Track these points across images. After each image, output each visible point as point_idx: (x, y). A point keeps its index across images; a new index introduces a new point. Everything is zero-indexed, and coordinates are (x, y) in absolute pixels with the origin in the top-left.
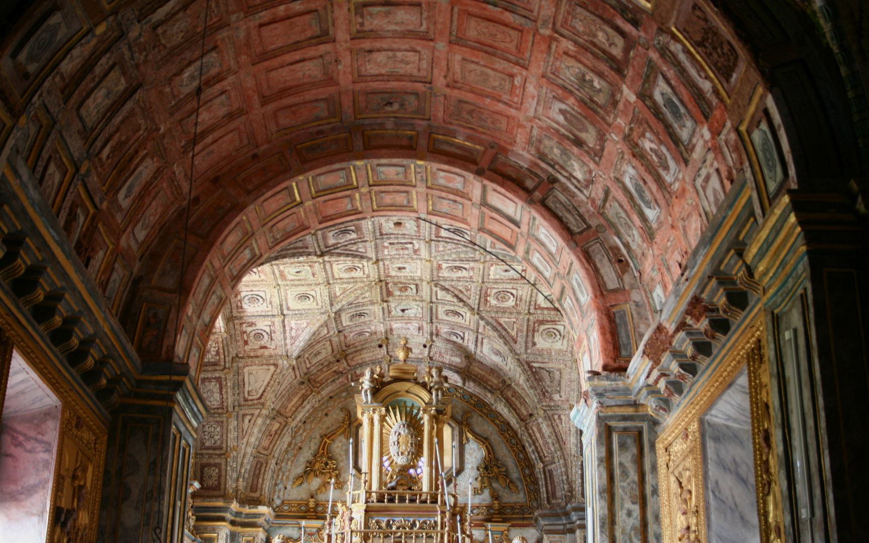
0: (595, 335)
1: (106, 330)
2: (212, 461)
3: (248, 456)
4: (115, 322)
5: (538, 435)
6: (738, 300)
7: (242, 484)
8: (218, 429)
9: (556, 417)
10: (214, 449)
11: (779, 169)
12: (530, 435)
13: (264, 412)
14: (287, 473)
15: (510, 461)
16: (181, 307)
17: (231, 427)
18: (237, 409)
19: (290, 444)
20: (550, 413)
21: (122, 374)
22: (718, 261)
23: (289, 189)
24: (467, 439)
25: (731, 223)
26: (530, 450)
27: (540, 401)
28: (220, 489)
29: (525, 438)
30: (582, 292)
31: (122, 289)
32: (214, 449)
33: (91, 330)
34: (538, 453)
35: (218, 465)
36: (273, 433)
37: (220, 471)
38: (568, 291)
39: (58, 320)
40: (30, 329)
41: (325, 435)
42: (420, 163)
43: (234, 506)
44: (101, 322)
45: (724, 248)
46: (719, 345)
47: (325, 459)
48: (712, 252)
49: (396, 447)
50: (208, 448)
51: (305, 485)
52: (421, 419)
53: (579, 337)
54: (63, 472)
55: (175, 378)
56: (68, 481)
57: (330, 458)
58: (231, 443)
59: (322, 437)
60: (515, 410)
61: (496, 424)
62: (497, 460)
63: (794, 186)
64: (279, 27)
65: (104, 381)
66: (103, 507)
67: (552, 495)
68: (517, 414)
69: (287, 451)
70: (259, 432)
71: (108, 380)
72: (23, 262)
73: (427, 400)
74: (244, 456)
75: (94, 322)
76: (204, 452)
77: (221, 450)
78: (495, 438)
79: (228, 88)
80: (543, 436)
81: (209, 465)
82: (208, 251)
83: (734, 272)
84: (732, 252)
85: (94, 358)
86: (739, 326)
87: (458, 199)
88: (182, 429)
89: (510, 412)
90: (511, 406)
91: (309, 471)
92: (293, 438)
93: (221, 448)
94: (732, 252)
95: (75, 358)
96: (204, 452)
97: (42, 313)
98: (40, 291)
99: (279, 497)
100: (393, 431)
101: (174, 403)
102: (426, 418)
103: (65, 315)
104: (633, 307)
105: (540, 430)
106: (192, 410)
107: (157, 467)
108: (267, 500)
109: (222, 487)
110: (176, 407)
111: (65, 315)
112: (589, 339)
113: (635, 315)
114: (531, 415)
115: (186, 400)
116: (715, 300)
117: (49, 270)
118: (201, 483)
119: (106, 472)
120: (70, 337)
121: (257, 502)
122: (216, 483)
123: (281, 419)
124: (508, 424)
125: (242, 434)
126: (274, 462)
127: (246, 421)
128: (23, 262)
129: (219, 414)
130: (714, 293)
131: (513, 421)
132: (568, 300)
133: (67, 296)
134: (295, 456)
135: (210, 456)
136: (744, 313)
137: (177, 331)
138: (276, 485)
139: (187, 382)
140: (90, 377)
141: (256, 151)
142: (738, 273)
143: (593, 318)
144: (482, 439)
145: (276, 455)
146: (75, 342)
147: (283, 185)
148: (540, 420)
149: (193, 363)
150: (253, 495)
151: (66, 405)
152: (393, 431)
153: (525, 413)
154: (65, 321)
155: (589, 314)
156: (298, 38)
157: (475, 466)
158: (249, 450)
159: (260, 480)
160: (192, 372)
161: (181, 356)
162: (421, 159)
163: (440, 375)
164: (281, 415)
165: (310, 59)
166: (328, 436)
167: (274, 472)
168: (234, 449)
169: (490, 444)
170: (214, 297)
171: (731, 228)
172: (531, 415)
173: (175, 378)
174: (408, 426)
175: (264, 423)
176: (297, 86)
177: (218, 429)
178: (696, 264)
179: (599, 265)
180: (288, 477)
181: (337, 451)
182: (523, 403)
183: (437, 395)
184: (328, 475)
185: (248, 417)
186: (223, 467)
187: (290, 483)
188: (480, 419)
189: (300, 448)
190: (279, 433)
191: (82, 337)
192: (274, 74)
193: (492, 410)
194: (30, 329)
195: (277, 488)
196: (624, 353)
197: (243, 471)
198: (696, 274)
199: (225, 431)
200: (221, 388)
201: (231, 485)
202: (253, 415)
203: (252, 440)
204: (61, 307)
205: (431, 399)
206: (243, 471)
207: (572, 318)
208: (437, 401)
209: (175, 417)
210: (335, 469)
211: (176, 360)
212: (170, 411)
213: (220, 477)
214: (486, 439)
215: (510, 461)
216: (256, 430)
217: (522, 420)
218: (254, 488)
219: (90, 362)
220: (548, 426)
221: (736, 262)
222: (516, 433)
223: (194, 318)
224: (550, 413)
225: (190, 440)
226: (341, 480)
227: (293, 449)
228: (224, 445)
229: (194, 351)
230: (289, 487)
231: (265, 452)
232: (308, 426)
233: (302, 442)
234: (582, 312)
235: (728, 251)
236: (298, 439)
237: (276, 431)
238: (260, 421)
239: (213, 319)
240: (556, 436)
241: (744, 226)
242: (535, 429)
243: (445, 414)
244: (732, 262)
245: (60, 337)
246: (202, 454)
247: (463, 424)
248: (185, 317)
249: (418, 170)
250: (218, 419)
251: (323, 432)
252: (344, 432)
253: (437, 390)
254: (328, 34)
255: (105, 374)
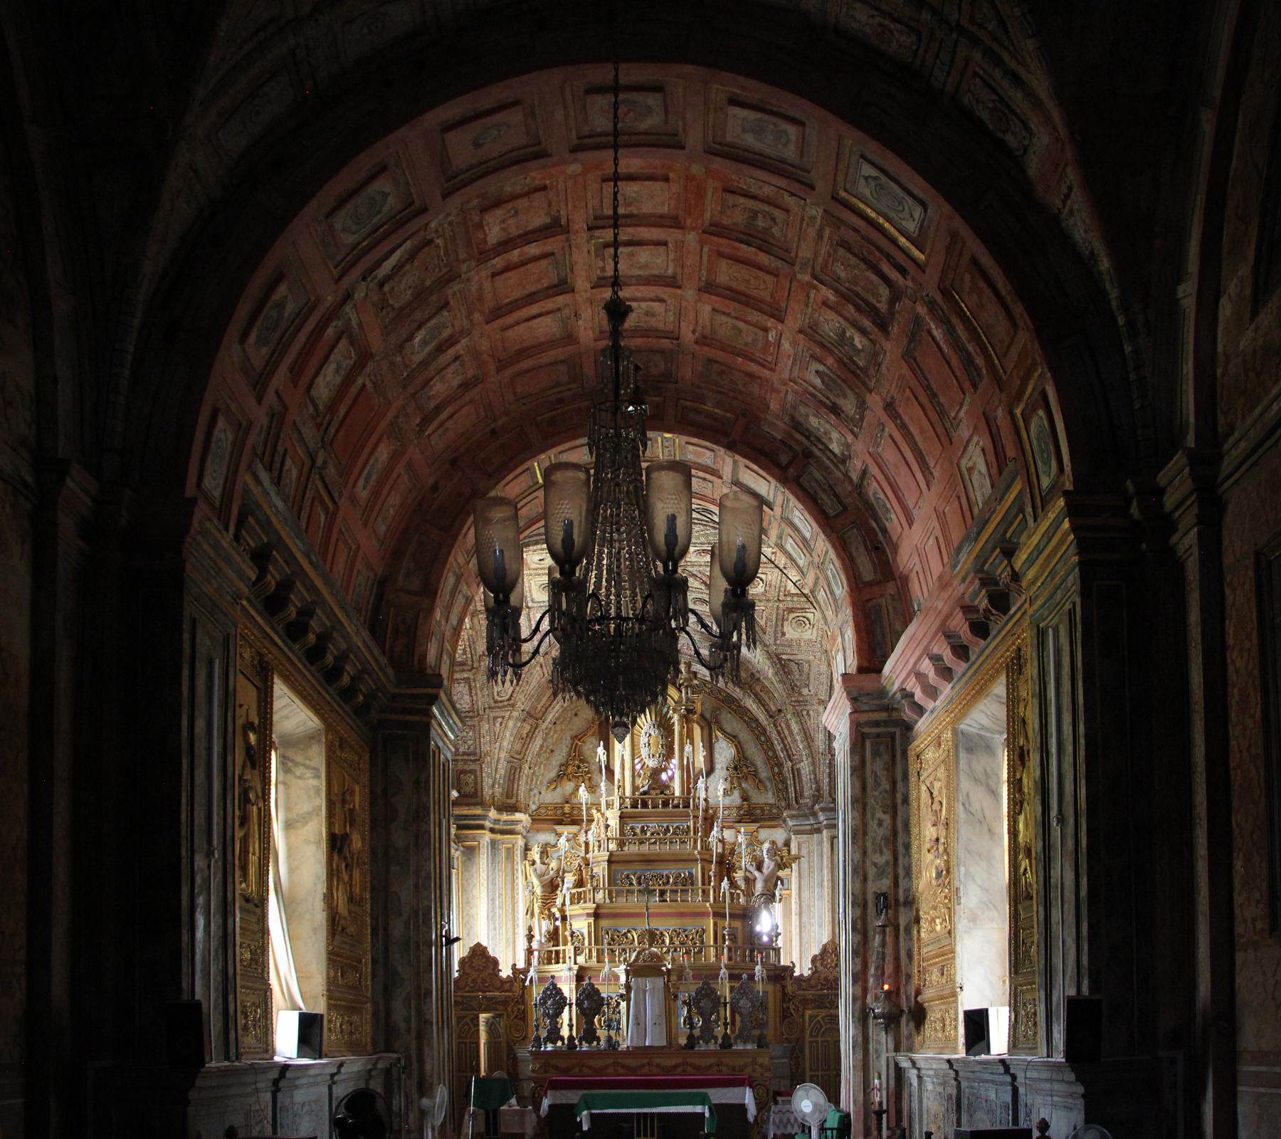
0: (850, 633)
1: (360, 644)
2: (466, 767)
3: (502, 761)
4: (365, 634)
5: (786, 732)
6: (1000, 601)
7: (498, 790)
8: (471, 734)
9: (805, 713)
10: (469, 755)
11: (1054, 463)
12: (778, 732)
13: (515, 714)
14: (540, 778)
15: (758, 759)
16: (430, 611)
17: (483, 731)
18: (487, 711)
19: (541, 747)
20: (799, 708)
21: (378, 689)
22: (981, 560)
23: (530, 470)
24: (716, 737)
25: (999, 518)
26: (778, 748)
27: (789, 696)
28: (477, 797)
29: (774, 736)
30: (837, 584)
31: (368, 592)
32: (469, 755)
33: (344, 646)
34: (787, 751)
35: (473, 772)
36: (525, 735)
37: (476, 777)
38: (822, 582)
39: (311, 637)
40: (286, 649)
41: (576, 737)
42: (667, 435)
43: (493, 814)
44: (353, 635)
45: (990, 546)
46: (977, 650)
47: (577, 762)
48: (978, 549)
49: (647, 749)
50: (464, 754)
51: (559, 789)
52: (671, 718)
53: (832, 635)
54: (334, 798)
55: (430, 691)
56: (338, 806)
57: (581, 761)
58: (485, 748)
59: (574, 738)
60: (763, 705)
61: (744, 721)
62: (746, 759)
63: (1069, 486)
64: (513, 276)
65: (361, 698)
66: (373, 827)
67: (799, 795)
68: (766, 710)
69: (539, 755)
70: (511, 735)
71: (365, 696)
72: (272, 579)
73: (676, 698)
74: (498, 761)
75: (346, 637)
76: (460, 758)
77: (475, 756)
78: (744, 735)
79: (462, 352)
80: (791, 733)
81: (464, 772)
82: (452, 546)
83: (998, 573)
84: (998, 550)
85: (349, 674)
86: (1000, 631)
87: (708, 476)
88: (441, 744)
89: (758, 708)
90: (760, 702)
91: (561, 776)
92: (545, 740)
93: (475, 754)
94: (998, 550)
95: (332, 675)
96: (460, 758)
97: (295, 631)
98: (293, 608)
99: (534, 803)
100: (643, 732)
101: (431, 718)
102: (676, 718)
103: (318, 631)
104: (889, 601)
105: (789, 727)
106: (448, 723)
107: (421, 785)
108: (523, 806)
109: (479, 794)
110: (433, 722)
111: (318, 631)
112: (843, 637)
113: (891, 610)
114: (780, 711)
115: (442, 713)
116: (976, 602)
117: (298, 584)
118: (459, 792)
119: (372, 792)
120: (324, 656)
121: (513, 809)
122: (473, 790)
123: (531, 721)
124: (757, 720)
125: (496, 738)
126: (527, 766)
127: (498, 725)
128: (272, 579)
129: (470, 717)
130: (976, 594)
131: (762, 717)
132: (822, 592)
133: (318, 611)
134: (548, 759)
135: (465, 761)
136: (1006, 618)
137: (428, 637)
138: (531, 790)
139: (442, 695)
140: (347, 694)
141: (493, 426)
142: (1003, 576)
143: (847, 613)
144: (733, 738)
145: (529, 759)
146: (330, 659)
147: (525, 466)
148: (789, 716)
149: (444, 672)
150: (509, 801)
151: (329, 727)
152: (643, 732)
153: (774, 709)
154: (319, 637)
155: (844, 608)
156: (533, 289)
157: (725, 766)
158: (503, 755)
159: (515, 786)
160: (445, 682)
161: (433, 665)
162: (668, 432)
163: (689, 671)
164: (531, 716)
165: (548, 313)
166: (578, 737)
167: (527, 777)
168: (487, 754)
169: (739, 742)
170: (460, 596)
171: (998, 524)
172: (780, 711)
173: (430, 691)
174: (659, 726)
175: (515, 725)
176: (534, 347)
177: (471, 734)
178: (959, 562)
179: (855, 554)
180: (541, 781)
181: (588, 753)
182: (772, 698)
183: (687, 693)
184: (581, 779)
185: (499, 720)
186: (478, 773)
187: (545, 788)
188: (729, 716)
189: (552, 751)
190: (530, 736)
191: (336, 653)
192: (510, 333)
193: (740, 706)
194: (286, 649)
195: (532, 793)
196: (879, 653)
197: (498, 777)
198: (958, 573)
199: (477, 735)
200: (470, 689)
201: (487, 791)
202: (503, 717)
203: (505, 744)
204: (313, 623)
205: (681, 697)
206: (498, 777)
207: (826, 613)
208: (688, 699)
209: (433, 733)
210: (588, 773)
211: (429, 671)
212: (427, 727)
213: (476, 783)
214: (735, 737)
215: (758, 759)
216: (508, 734)
217: (771, 717)
218: (509, 793)
219: (346, 679)
220: (797, 723)
221: (1002, 561)
222: (765, 730)
223: (443, 622)
224: (799, 708)
225: (448, 754)
226: (593, 783)
227: (545, 752)
228: (478, 751)
229: (445, 657)
230: (543, 792)
231: (518, 757)
232: (558, 727)
233: (554, 744)
234: (836, 606)
235: (993, 550)
236: (550, 740)
237: (527, 734)
238: (511, 724)
239: (461, 621)
240: (805, 733)
241: (1011, 523)
242: (783, 726)
243: (695, 713)
244: (997, 561)
245: (314, 655)
246: (457, 760)
247: (710, 725)
248: (434, 622)
249: (666, 444)
250: (469, 723)
251: (574, 733)
252: (593, 734)
253: (687, 687)
254: (566, 282)
255: (362, 692)
